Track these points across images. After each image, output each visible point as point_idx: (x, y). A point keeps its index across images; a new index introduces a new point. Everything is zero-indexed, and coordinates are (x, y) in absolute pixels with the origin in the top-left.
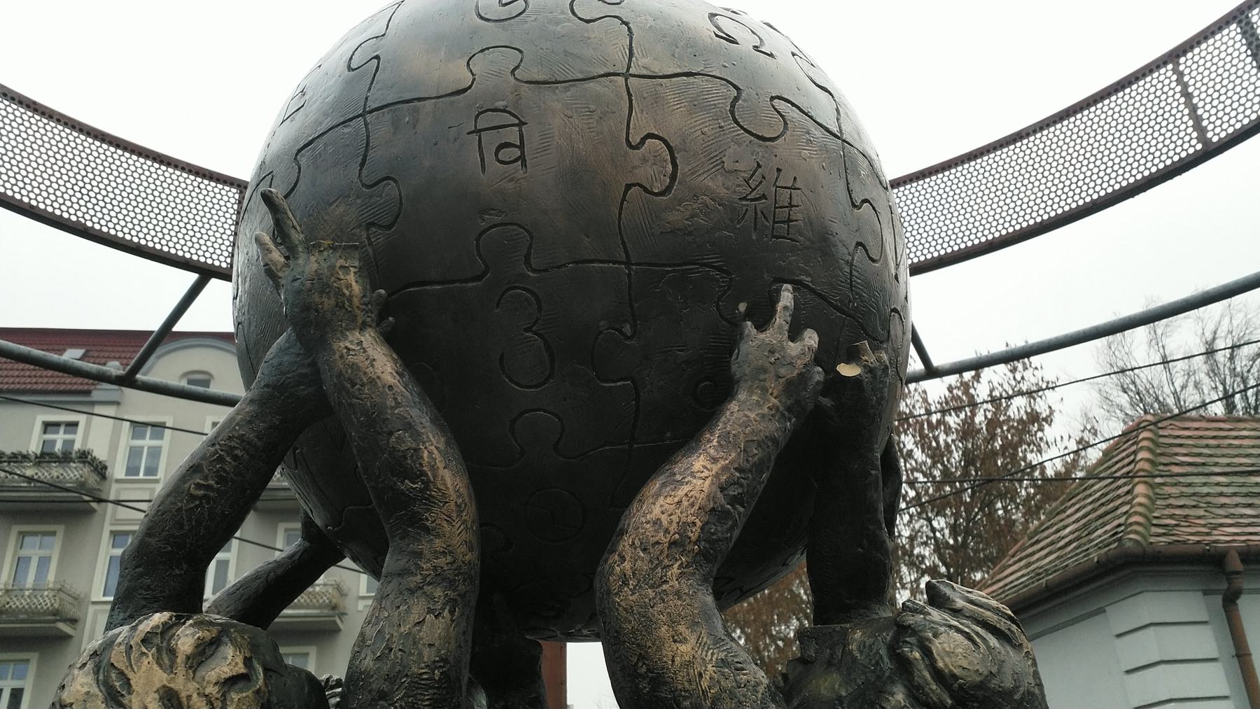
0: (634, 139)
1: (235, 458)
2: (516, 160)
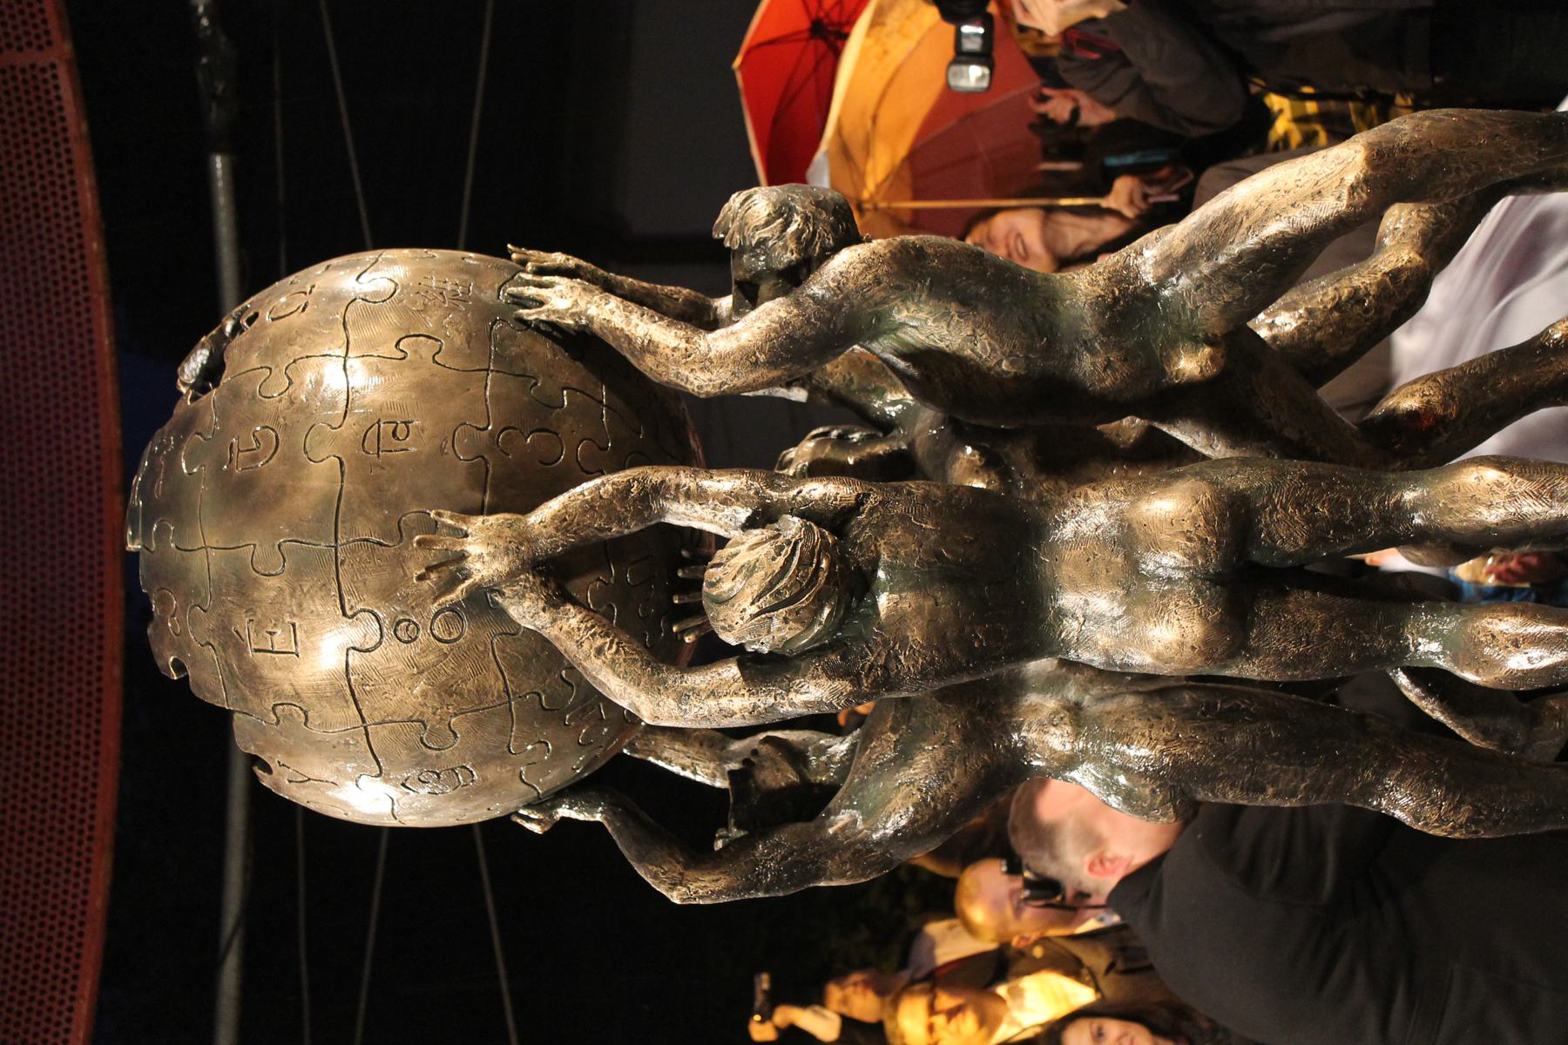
0: (401, 355)
1: (593, 627)
2: (408, 428)
